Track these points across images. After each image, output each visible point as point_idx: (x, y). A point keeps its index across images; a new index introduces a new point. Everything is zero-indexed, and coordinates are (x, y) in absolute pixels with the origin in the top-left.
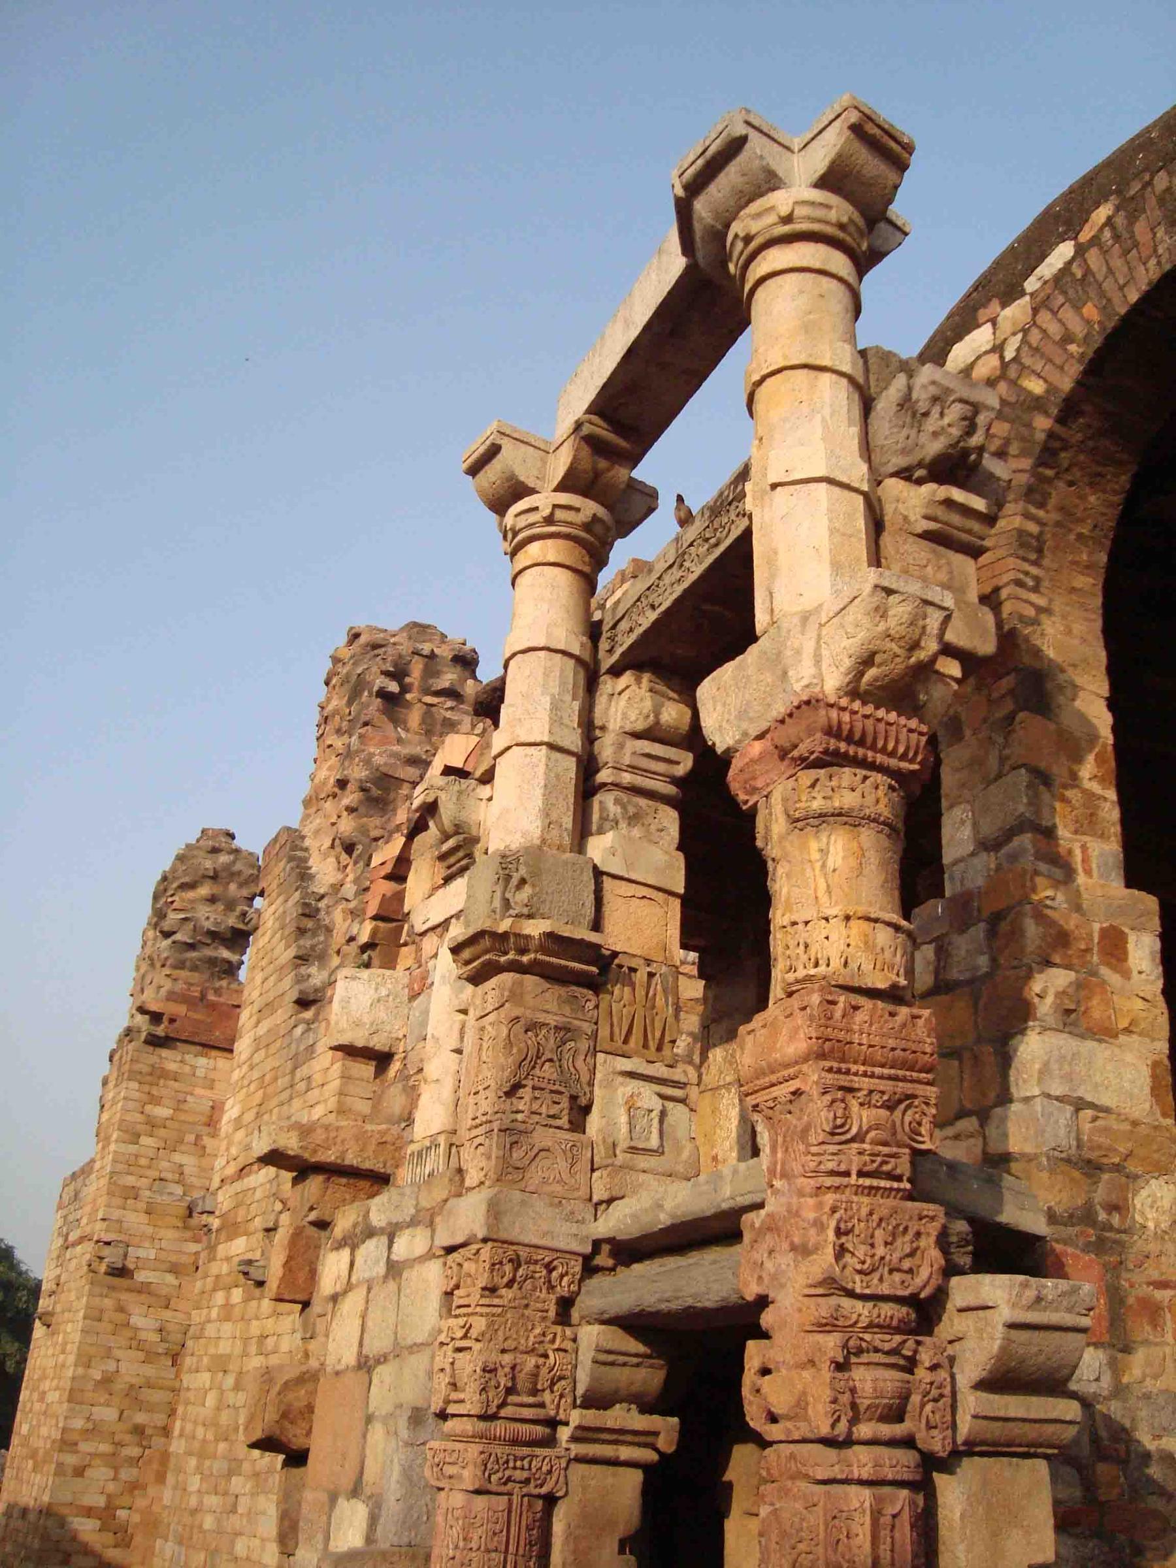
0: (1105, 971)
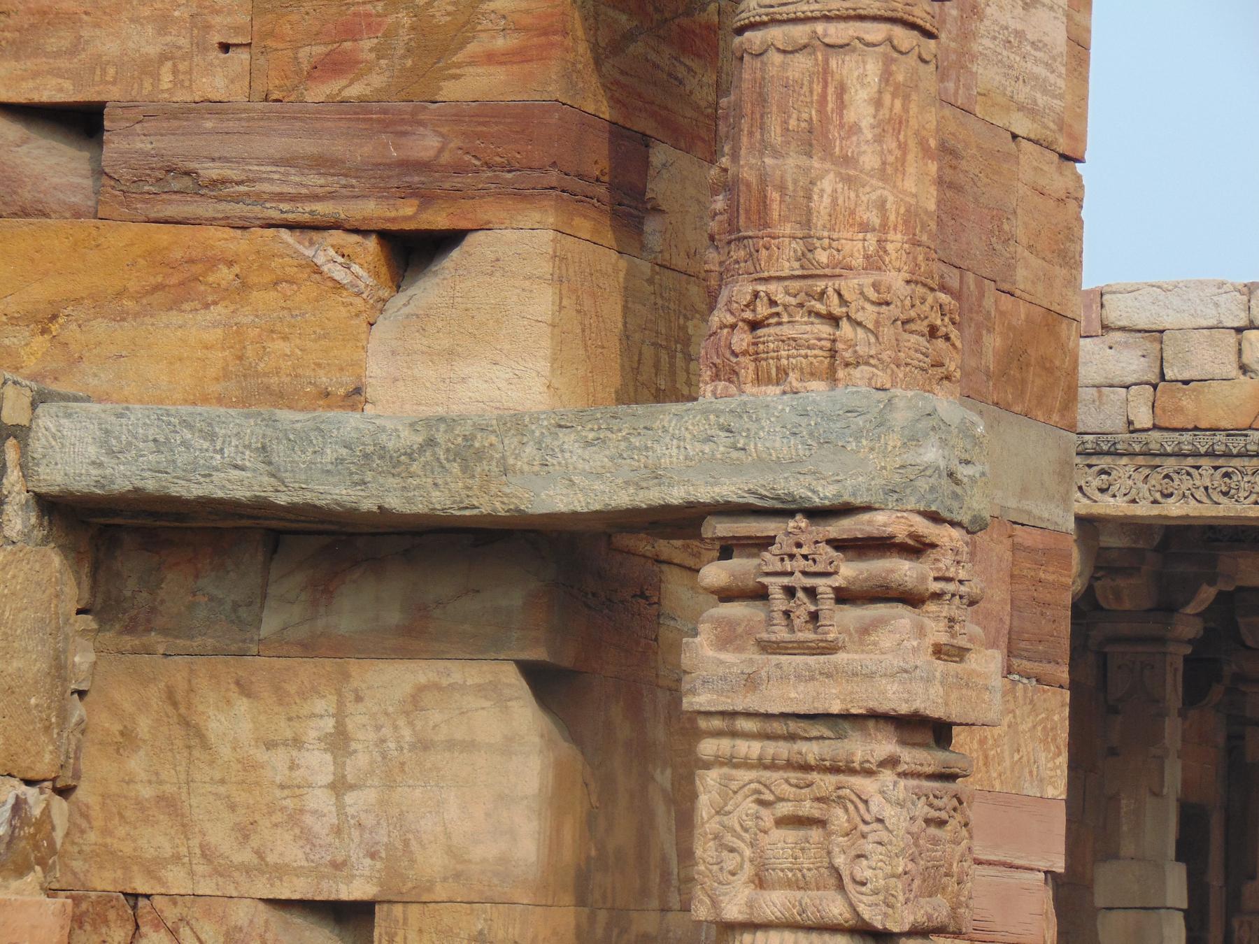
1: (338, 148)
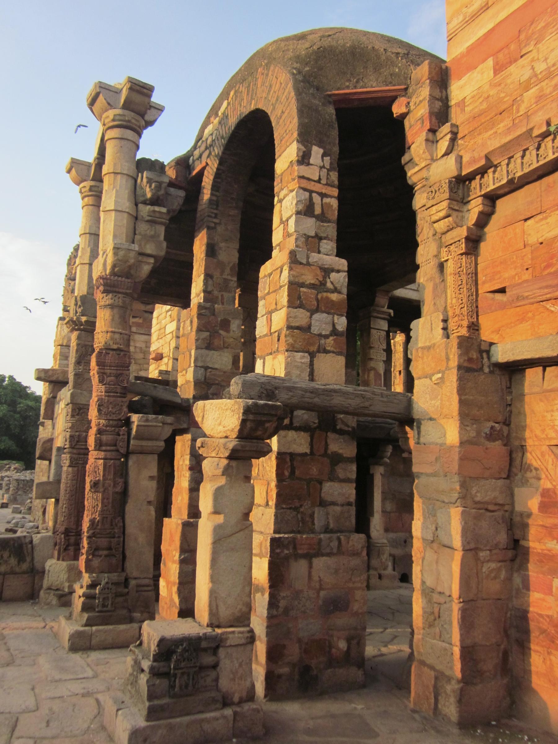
0: (221, 332)
1: (550, 283)
